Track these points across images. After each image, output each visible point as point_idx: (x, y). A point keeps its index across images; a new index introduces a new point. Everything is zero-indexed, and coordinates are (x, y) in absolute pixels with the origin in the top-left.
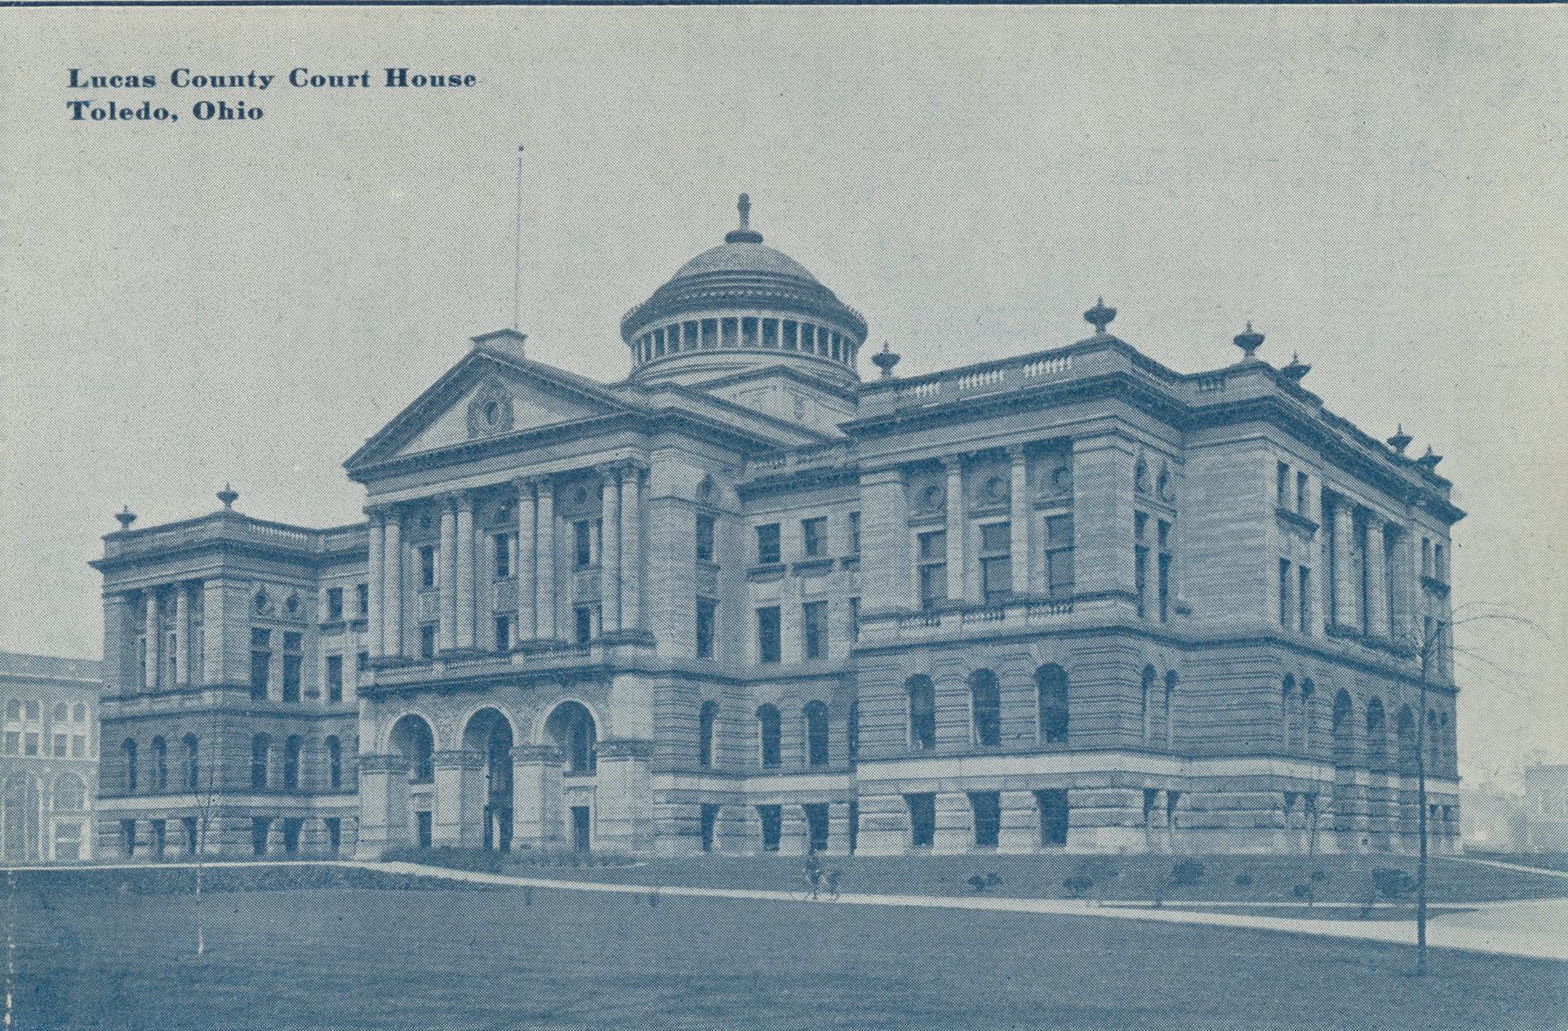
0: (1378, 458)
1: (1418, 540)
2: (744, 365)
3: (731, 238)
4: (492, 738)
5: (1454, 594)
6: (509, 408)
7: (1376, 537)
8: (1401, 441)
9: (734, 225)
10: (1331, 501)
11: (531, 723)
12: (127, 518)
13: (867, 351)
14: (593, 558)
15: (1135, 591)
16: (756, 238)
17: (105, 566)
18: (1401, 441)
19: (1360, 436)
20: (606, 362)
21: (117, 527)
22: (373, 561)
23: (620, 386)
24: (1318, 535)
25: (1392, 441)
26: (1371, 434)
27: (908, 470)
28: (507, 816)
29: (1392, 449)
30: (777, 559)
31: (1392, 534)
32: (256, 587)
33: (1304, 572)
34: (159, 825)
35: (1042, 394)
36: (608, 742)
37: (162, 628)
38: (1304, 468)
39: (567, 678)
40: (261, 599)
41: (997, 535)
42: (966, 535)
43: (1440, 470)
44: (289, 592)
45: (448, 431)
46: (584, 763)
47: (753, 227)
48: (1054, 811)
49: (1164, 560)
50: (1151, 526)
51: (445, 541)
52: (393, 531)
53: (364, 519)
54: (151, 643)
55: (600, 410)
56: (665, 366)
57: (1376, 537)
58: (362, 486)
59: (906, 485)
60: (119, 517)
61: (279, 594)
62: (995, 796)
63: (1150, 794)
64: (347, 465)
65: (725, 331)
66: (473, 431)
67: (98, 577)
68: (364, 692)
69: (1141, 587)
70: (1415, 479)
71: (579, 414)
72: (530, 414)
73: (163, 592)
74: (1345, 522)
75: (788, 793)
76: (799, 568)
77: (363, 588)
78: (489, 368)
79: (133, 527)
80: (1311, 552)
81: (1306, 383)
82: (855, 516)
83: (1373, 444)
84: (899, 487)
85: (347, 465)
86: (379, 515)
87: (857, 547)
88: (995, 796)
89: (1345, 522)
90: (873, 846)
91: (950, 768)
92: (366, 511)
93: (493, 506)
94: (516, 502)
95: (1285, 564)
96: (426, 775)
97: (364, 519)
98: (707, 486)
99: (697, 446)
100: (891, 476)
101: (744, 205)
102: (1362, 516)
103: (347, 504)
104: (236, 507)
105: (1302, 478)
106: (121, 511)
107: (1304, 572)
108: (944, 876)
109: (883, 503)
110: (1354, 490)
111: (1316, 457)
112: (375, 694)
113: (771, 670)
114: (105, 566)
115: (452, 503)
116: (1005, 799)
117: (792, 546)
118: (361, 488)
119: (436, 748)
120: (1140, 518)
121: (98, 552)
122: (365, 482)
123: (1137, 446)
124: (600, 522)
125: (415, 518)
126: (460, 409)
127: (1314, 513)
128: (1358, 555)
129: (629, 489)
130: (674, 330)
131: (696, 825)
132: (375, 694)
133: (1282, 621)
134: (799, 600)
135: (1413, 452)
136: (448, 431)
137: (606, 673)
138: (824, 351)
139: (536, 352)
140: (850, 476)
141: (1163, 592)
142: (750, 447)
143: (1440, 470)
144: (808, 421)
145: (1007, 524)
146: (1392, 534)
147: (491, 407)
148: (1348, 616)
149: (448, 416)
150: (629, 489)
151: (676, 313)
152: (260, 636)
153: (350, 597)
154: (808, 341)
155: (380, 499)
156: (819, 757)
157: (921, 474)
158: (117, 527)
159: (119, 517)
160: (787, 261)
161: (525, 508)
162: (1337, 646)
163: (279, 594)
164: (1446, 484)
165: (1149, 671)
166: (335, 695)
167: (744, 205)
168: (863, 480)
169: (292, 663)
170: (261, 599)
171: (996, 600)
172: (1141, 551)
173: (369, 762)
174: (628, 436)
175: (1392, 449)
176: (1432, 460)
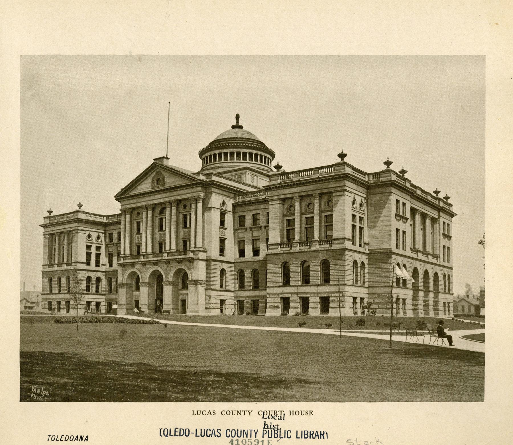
0: (429, 198)
1: (442, 223)
2: (237, 166)
3: (233, 127)
4: (158, 279)
5: (453, 239)
6: (164, 180)
7: (428, 222)
8: (437, 192)
9: (235, 124)
10: (413, 211)
11: (169, 275)
12: (50, 212)
13: (274, 163)
14: (188, 226)
15: (351, 238)
16: (241, 127)
17: (44, 226)
18: (437, 192)
19: (423, 191)
20: (192, 165)
21: (48, 214)
22: (122, 226)
23: (198, 174)
24: (409, 220)
25: (434, 192)
26: (426, 190)
28: (162, 301)
29: (435, 195)
30: (245, 226)
31: (434, 221)
32: (87, 233)
33: (404, 232)
34: (59, 303)
35: (271, 187)
36: (192, 281)
38: (405, 201)
39: (180, 261)
40: (89, 236)
41: (310, 221)
42: (301, 220)
43: (449, 201)
44: (96, 234)
45: (146, 186)
46: (185, 287)
47: (240, 123)
48: (325, 303)
49: (361, 229)
50: (358, 219)
51: (144, 219)
52: (128, 216)
53: (120, 212)
54: (57, 250)
55: (191, 181)
56: (208, 167)
57: (428, 222)
58: (119, 203)
59: (283, 204)
60: (48, 212)
61: (94, 235)
62: (307, 298)
63: (355, 299)
65: (237, 156)
66: (153, 187)
67: (42, 229)
68: (119, 265)
69: (353, 236)
70: (442, 204)
71: (184, 182)
72: (170, 181)
74: (418, 217)
75: (246, 297)
76: (251, 228)
77: (119, 233)
78: (158, 168)
79: (52, 214)
80: (407, 227)
81: (406, 176)
82: (268, 213)
83: (426, 193)
84: (281, 205)
86: (124, 211)
87: (268, 223)
88: (307, 298)
89: (418, 217)
90: (271, 313)
92: (121, 210)
94: (165, 208)
95: (398, 230)
96: (138, 289)
97: (120, 212)
98: (224, 203)
99: (220, 192)
100: (278, 202)
101: (238, 117)
102: (424, 216)
103: (116, 208)
104: (82, 209)
105: (404, 204)
106: (49, 210)
107: (404, 232)
108: (291, 323)
109: (275, 210)
110: (421, 207)
111: (408, 198)
112: (123, 266)
114: (44, 226)
115: (146, 208)
116: (311, 299)
117: (249, 222)
119: (141, 281)
120: (354, 216)
121: (42, 222)
122: (120, 202)
123: (353, 195)
124: (190, 214)
126: (149, 180)
127: (408, 215)
128: (422, 227)
129: (200, 205)
130: (215, 155)
131: (219, 306)
132: (123, 266)
133: (397, 248)
134: (251, 238)
135: (441, 196)
138: (261, 161)
139: (171, 163)
140: (266, 201)
141: (361, 238)
142: (237, 193)
143: (449, 201)
144: (255, 184)
145: (313, 217)
146: (434, 221)
147: (158, 180)
148: (419, 246)
149: (146, 182)
150: (200, 205)
151: (215, 151)
152: (89, 247)
153: (115, 236)
154: (256, 160)
155: (124, 207)
156: (256, 287)
158: (48, 214)
159: (48, 212)
160: (252, 135)
161: (168, 210)
162: (414, 255)
163: (94, 235)
164: (450, 205)
165: (355, 262)
166: (111, 266)
167: (238, 117)
168: (270, 203)
169: (98, 256)
170: (89, 236)
171: (308, 239)
172: (354, 226)
173: (122, 285)
174: (199, 189)
175: (435, 195)
176: (447, 198)
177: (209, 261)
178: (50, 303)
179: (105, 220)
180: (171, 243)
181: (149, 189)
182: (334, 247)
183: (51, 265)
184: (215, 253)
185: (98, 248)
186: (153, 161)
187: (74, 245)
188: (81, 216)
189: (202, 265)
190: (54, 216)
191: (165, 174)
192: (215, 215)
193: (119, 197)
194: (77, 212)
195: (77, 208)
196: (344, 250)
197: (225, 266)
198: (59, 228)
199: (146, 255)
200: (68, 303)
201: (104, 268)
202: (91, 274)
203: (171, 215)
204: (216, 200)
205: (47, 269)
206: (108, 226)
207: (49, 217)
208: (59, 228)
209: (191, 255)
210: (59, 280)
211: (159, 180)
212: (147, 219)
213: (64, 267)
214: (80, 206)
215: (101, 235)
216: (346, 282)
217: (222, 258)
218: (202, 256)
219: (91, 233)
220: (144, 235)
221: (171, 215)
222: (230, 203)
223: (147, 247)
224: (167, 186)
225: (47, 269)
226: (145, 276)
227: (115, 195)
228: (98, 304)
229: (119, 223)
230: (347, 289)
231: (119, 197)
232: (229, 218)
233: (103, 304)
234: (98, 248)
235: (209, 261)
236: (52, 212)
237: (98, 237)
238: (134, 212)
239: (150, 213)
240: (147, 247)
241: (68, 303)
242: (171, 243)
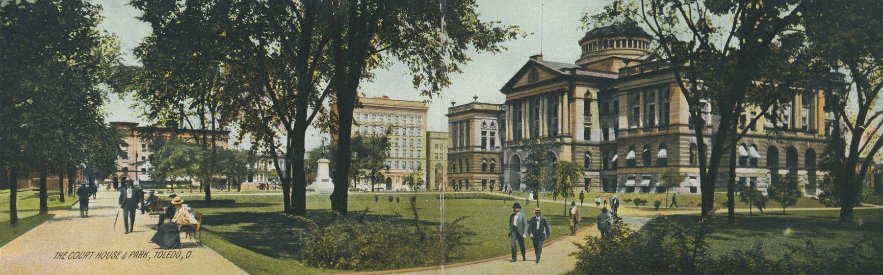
12: (453, 103)
17: (448, 116)
27: (630, 91)
34: (460, 182)
37: (461, 130)
40: (484, 124)
45: (524, 81)
52: (512, 107)
67: (447, 118)
72: (543, 76)
73: (461, 122)
86: (508, 103)
91: (638, 171)
93: (533, 101)
98: (588, 93)
103: (502, 99)
104: (478, 100)
113: (588, 142)
114: (448, 116)
126: (526, 76)
129: (566, 97)
136: (524, 81)
137: (559, 145)
152: (484, 133)
157: (630, 91)
158: (451, 106)
170: (484, 124)
177: (574, 145)
178: (454, 182)
179: (498, 108)
180: (544, 130)
182: (670, 132)
183: (454, 149)
184: (580, 137)
185: (492, 134)
186: (529, 59)
187: (471, 132)
188: (477, 107)
189: (567, 149)
191: (539, 71)
192: (580, 105)
193: (504, 90)
194: (473, 103)
195: (474, 100)
196: (680, 134)
197: (590, 149)
198: (460, 118)
199: (525, 141)
200: (467, 181)
201: (498, 150)
202: (486, 156)
203: (543, 104)
204: (580, 91)
205: (452, 152)
206: (498, 113)
208: (460, 118)
209: (558, 140)
210: (460, 161)
211: (534, 76)
212: (526, 108)
213: (465, 150)
214: (476, 98)
215: (495, 122)
216: (681, 163)
217: (588, 142)
218: (568, 140)
219: (486, 121)
220: (523, 123)
221: (543, 104)
222: (594, 94)
223: (526, 133)
224: (540, 80)
225: (452, 152)
226: (524, 156)
228: (493, 181)
229: (505, 111)
230: (682, 170)
231: (504, 90)
232: (594, 106)
233: (497, 181)
234: (492, 134)
235: (574, 145)
237: (492, 124)
238: (515, 103)
239: (528, 105)
240: (526, 133)
241: (467, 181)
242: (544, 130)
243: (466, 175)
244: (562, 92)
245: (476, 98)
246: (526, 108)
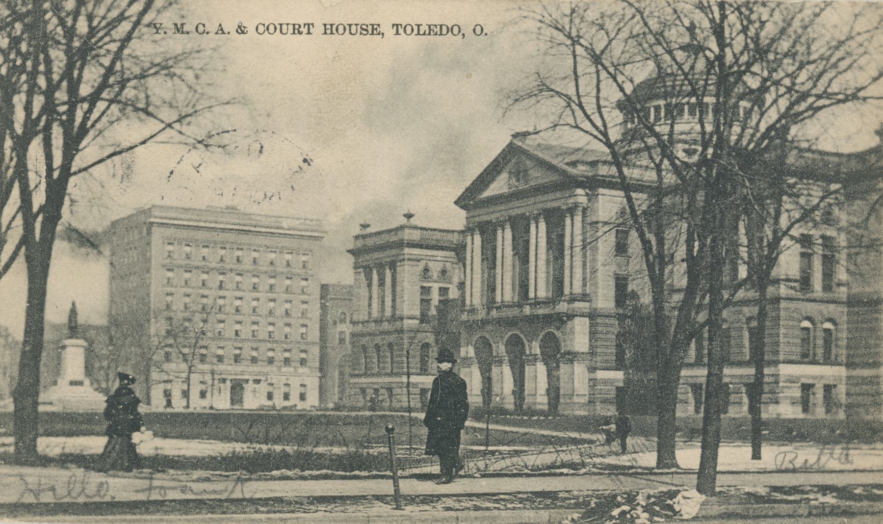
12: (365, 226)
37: (382, 284)
45: (499, 186)
52: (478, 239)
64: (456, 203)
67: (351, 259)
72: (538, 177)
79: (369, 230)
85: (456, 203)
86: (469, 230)
104: (413, 221)
118: (463, 213)
121: (351, 246)
125: (488, 231)
129: (578, 218)
136: (499, 186)
150: (578, 218)
152: (425, 290)
170: (426, 270)
181: (505, 190)
186: (508, 140)
189: (581, 326)
190: (371, 235)
193: (460, 202)
194: (402, 228)
195: (403, 221)
207: (364, 237)
219: (431, 265)
227: (454, 200)
231: (460, 202)
235: (593, 316)
236: (368, 226)
243: (387, 380)
244: (572, 211)
245: (409, 216)
246: (505, 238)
